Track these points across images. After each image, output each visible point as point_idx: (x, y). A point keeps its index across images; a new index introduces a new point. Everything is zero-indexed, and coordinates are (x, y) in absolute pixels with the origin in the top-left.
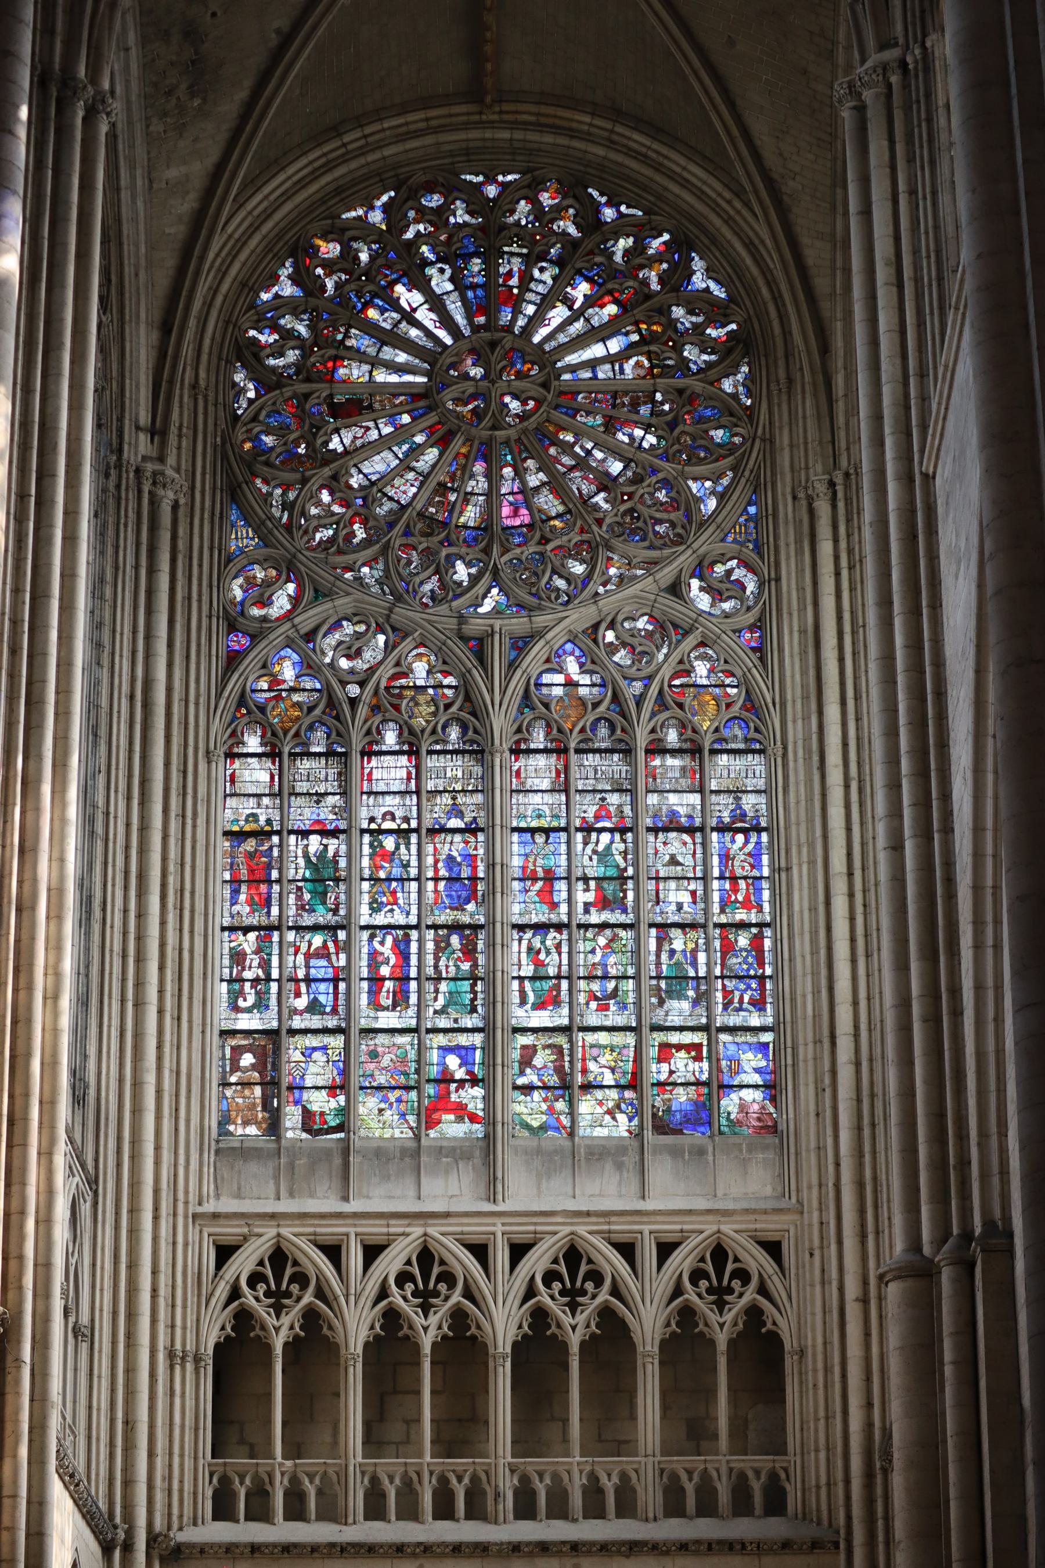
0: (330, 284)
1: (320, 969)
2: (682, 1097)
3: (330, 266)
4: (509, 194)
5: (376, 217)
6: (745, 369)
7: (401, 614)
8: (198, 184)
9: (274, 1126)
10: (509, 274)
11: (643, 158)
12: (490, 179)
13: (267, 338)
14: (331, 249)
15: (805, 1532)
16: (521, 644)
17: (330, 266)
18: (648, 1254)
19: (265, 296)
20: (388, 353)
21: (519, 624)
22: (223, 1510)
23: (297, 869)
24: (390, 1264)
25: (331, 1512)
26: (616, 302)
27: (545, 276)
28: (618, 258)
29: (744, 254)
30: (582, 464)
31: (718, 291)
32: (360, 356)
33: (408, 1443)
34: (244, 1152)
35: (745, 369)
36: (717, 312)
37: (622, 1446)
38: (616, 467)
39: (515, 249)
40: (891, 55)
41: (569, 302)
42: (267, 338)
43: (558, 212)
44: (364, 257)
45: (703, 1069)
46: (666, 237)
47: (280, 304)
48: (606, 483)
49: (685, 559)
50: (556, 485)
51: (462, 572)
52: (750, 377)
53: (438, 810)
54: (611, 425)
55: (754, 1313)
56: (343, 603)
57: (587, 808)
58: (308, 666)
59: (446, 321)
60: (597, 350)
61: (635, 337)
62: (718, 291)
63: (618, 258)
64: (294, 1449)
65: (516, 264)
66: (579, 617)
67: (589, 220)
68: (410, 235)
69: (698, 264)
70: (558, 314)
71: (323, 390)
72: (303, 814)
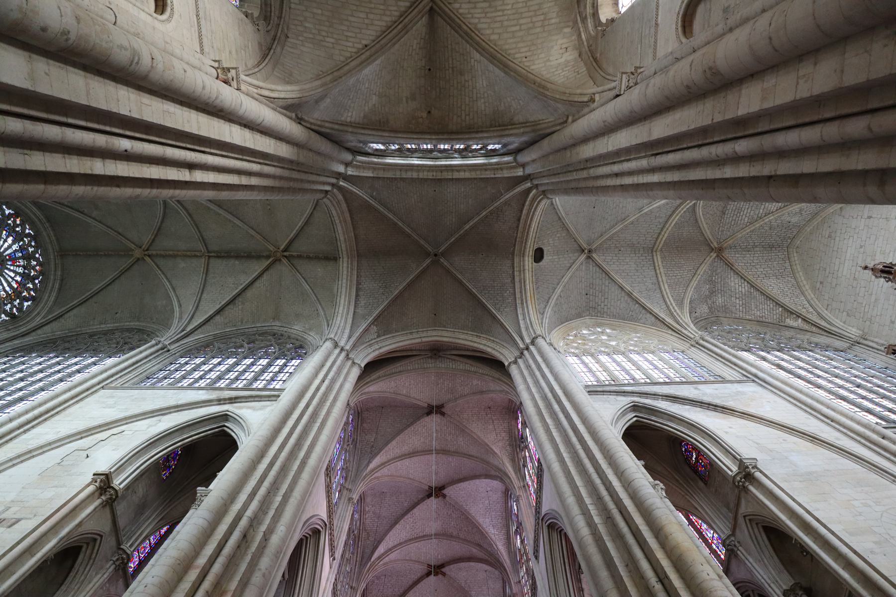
0: (10, 222)
3: (14, 222)
4: (37, 260)
5: (27, 231)
6: (7, 319)
10: (19, 262)
11: (53, 287)
12: (40, 255)
17: (14, 222)
19: (4, 207)
26: (18, 287)
27: (20, 270)
28: (28, 285)
29: (36, 313)
35: (7, 319)
36: (20, 309)
39: (26, 262)
41: (15, 276)
43: (36, 271)
44: (17, 229)
46: (34, 295)
52: (6, 320)
59: (6, 250)
60: (5, 285)
61: (10, 293)
63: (28, 285)
65: (22, 263)
67: (36, 277)
68: (25, 239)
69: (29, 303)
70: (12, 275)
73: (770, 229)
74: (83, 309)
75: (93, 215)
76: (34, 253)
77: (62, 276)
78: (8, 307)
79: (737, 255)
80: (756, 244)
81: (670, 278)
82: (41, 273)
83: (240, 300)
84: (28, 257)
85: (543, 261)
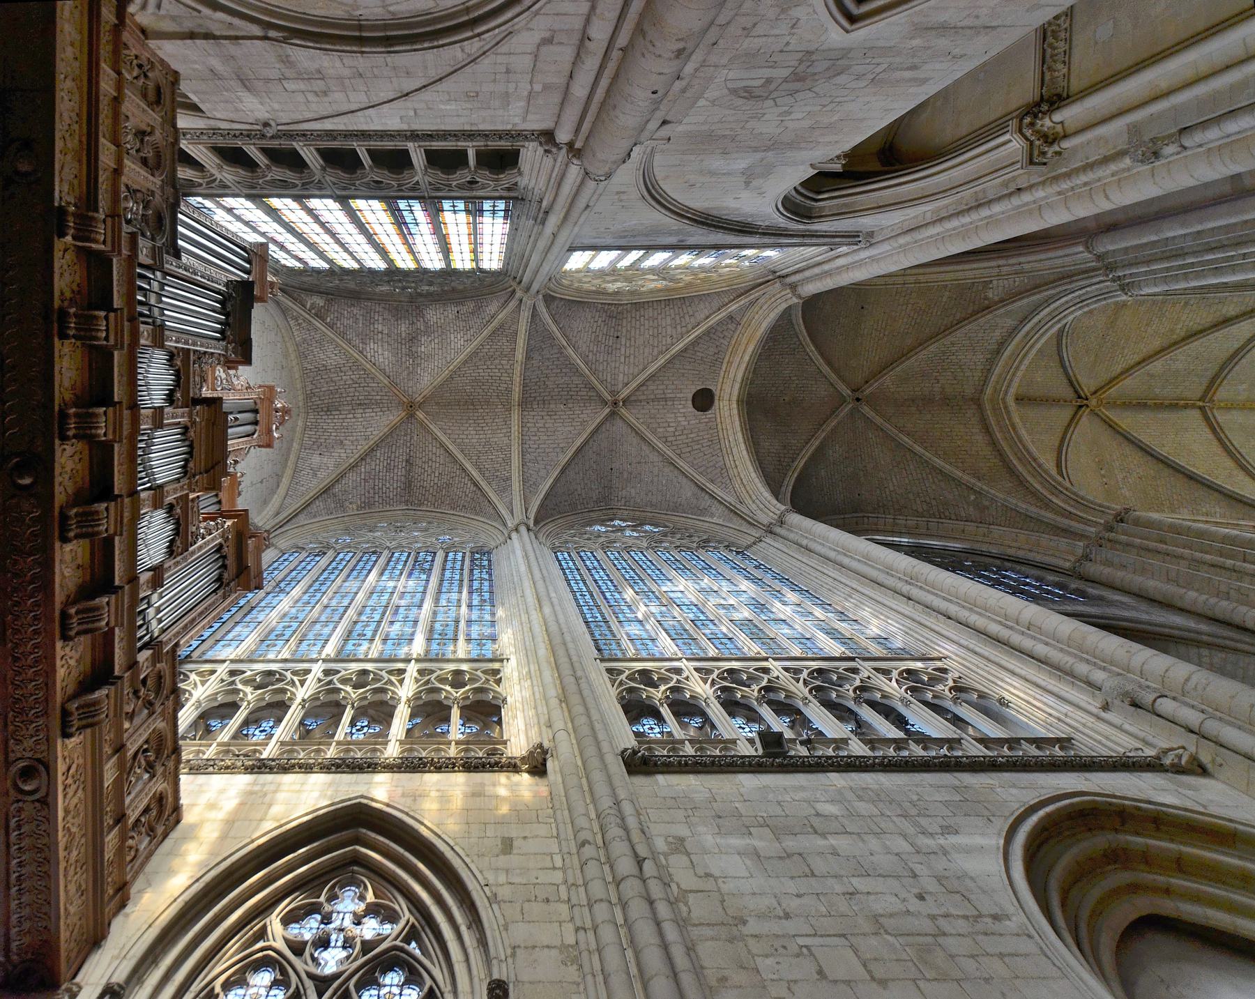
73: (342, 442)
79: (378, 397)
80: (351, 416)
81: (500, 367)
85: (694, 391)
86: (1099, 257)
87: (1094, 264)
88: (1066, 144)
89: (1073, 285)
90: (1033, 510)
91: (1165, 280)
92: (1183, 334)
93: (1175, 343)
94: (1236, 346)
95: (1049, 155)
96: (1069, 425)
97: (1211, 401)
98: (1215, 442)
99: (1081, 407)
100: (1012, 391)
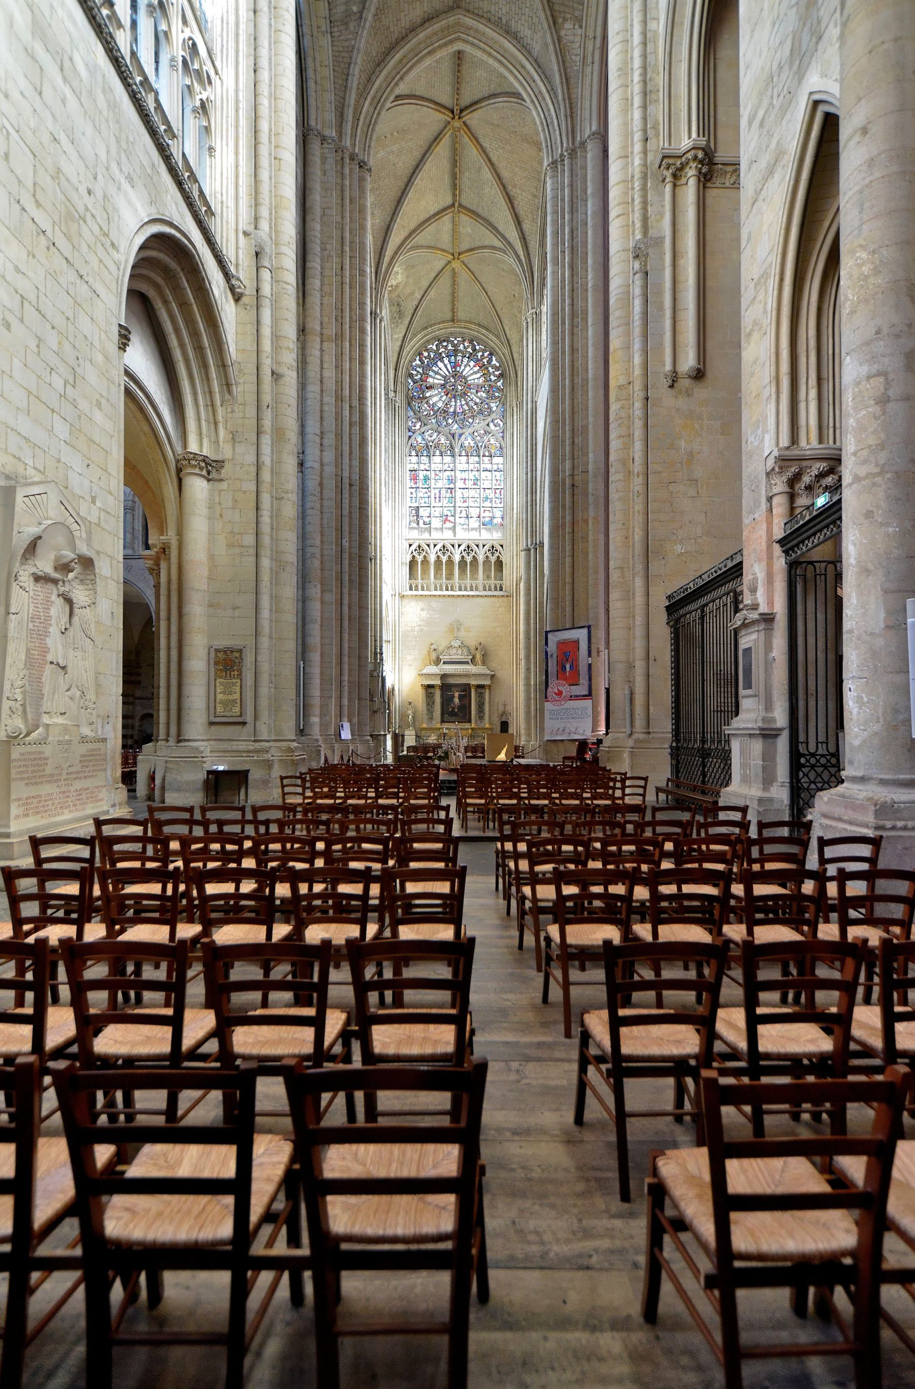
1: (426, 495)
2: (487, 519)
5: (434, 347)
7: (440, 429)
8: (401, 339)
9: (418, 524)
11: (484, 335)
13: (414, 372)
14: (426, 354)
15: (506, 594)
16: (460, 435)
18: (481, 546)
20: (437, 376)
21: (460, 431)
22: (411, 589)
23: (421, 477)
24: (438, 548)
25: (428, 590)
27: (466, 360)
30: (472, 400)
31: (498, 365)
32: (432, 377)
33: (441, 578)
34: (413, 528)
36: (497, 369)
37: (476, 579)
38: (478, 400)
40: (534, 310)
42: (414, 372)
45: (491, 515)
47: (417, 366)
48: (476, 404)
49: (490, 419)
50: (467, 404)
51: (450, 421)
53: (446, 467)
54: (477, 392)
55: (498, 557)
56: (429, 427)
57: (471, 467)
58: (424, 439)
62: (498, 365)
64: (422, 579)
66: (470, 430)
67: (474, 350)
69: (494, 358)
70: (468, 368)
71: (425, 384)
72: (422, 467)
74: (506, 322)
75: (419, 297)
76: (454, 345)
77: (476, 324)
78: (493, 378)
82: (471, 342)
83: (510, 188)
84: (456, 352)
86: (583, 144)
87: (578, 139)
88: (668, 188)
89: (563, 118)
90: (354, 83)
91: (555, 197)
92: (511, 193)
93: (504, 187)
94: (500, 228)
95: (665, 172)
96: (436, 103)
97: (459, 212)
98: (427, 216)
99: (453, 112)
100: (468, 48)
